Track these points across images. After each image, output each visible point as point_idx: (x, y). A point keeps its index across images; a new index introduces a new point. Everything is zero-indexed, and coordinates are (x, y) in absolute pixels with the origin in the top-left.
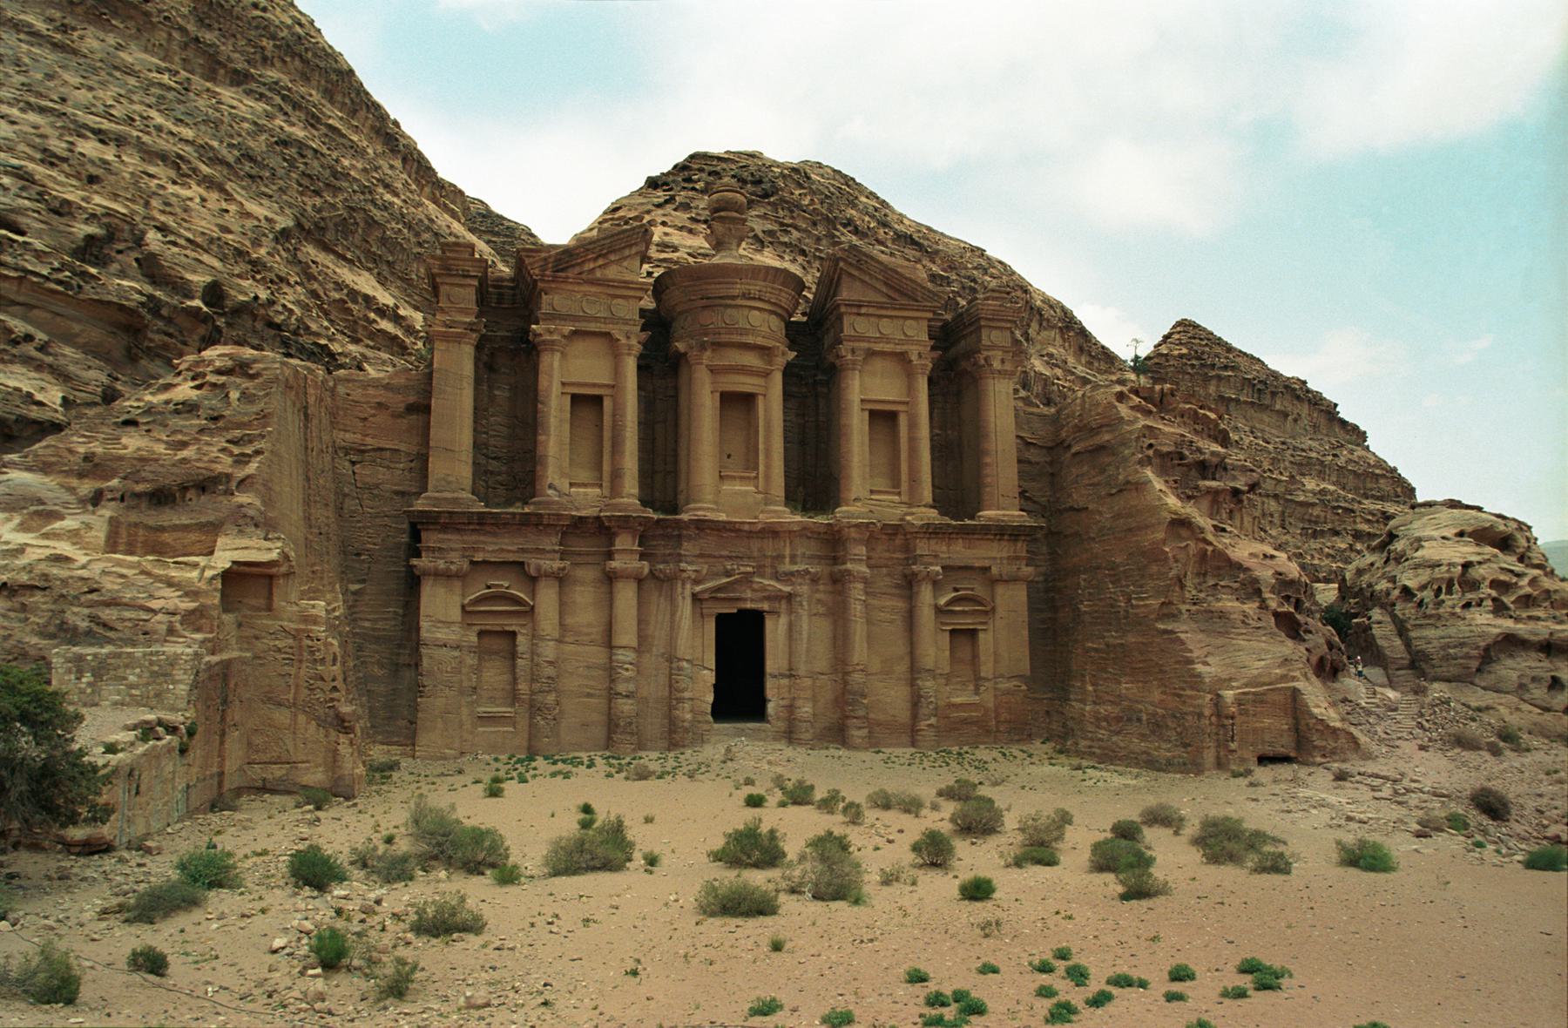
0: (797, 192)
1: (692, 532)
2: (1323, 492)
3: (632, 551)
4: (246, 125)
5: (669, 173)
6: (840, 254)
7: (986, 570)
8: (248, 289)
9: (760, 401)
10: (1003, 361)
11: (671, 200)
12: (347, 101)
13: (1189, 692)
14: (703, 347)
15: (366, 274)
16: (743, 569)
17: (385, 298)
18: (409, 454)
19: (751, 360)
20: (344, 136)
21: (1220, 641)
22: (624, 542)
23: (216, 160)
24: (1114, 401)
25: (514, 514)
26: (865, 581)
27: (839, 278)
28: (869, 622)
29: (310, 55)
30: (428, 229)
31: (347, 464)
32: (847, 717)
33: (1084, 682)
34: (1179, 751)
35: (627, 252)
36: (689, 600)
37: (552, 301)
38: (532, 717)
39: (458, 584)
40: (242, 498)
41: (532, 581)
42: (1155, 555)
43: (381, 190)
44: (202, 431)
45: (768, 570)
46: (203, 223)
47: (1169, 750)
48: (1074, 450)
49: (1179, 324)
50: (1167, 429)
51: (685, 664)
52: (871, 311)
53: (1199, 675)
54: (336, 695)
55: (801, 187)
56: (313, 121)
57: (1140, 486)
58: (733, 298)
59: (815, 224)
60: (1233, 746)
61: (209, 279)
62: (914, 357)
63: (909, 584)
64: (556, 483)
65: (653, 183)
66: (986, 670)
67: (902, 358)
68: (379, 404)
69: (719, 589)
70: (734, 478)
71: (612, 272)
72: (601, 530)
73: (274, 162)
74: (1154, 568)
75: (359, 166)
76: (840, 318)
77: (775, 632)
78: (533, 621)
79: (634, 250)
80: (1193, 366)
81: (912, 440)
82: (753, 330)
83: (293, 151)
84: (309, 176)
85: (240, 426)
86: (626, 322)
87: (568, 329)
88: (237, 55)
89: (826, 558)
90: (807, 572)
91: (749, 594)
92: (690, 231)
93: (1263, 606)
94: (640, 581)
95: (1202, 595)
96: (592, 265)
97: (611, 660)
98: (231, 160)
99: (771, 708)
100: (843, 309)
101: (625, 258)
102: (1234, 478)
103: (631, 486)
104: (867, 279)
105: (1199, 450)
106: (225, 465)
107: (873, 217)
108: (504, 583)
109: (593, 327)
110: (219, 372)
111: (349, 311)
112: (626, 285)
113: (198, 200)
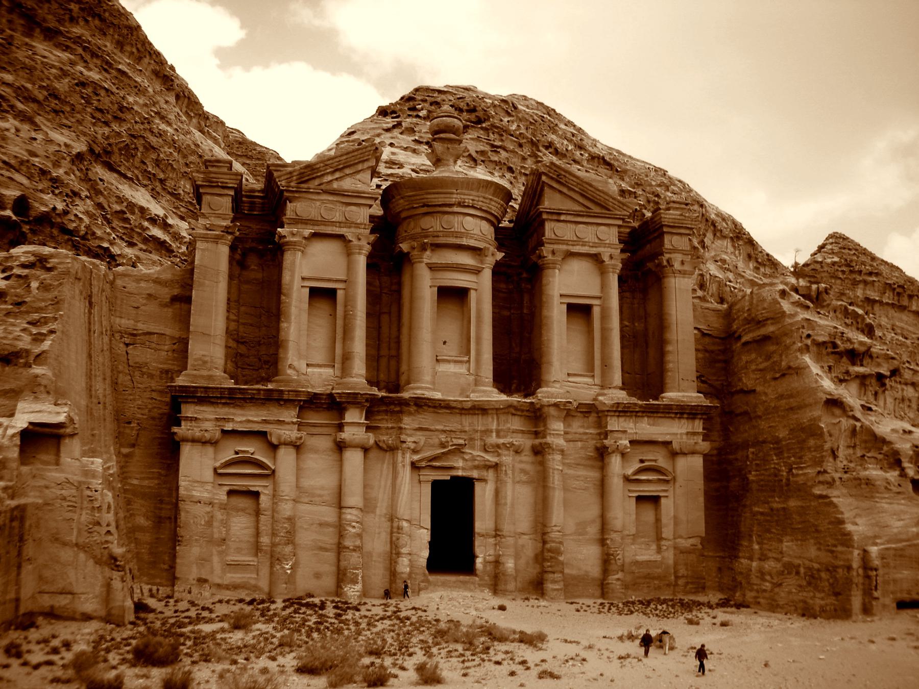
0: (506, 120)
1: (413, 409)
3: (359, 424)
4: (54, 71)
5: (397, 103)
6: (542, 169)
7: (667, 444)
8: (50, 202)
9: (473, 295)
10: (683, 263)
11: (399, 124)
12: (134, 50)
13: (840, 548)
14: (423, 248)
15: (143, 190)
16: (456, 441)
17: (157, 209)
18: (172, 338)
19: (465, 259)
20: (130, 78)
21: (866, 504)
22: (353, 416)
23: (29, 98)
24: (777, 297)
25: (259, 390)
26: (562, 452)
27: (542, 190)
28: (565, 489)
29: (107, 14)
30: (194, 152)
31: (122, 345)
32: (546, 572)
33: (751, 541)
34: (831, 600)
35: (360, 167)
36: (408, 468)
38: (272, 566)
39: (210, 450)
40: (37, 370)
41: (274, 448)
42: (813, 431)
43: (157, 121)
44: (8, 314)
45: (478, 443)
46: (17, 149)
47: (822, 599)
48: (744, 339)
49: (832, 236)
50: (822, 322)
51: (405, 524)
52: (569, 218)
53: (849, 534)
54: (110, 538)
55: (509, 114)
56: (107, 67)
57: (799, 371)
58: (451, 205)
59: (521, 146)
60: (876, 594)
61: (18, 193)
62: (606, 258)
63: (602, 454)
64: (295, 364)
65: (383, 112)
66: (668, 531)
67: (596, 258)
68: (150, 295)
69: (435, 458)
70: (448, 361)
71: (348, 184)
72: (332, 405)
73: (75, 99)
74: (812, 442)
75: (141, 102)
76: (542, 223)
77: (483, 496)
78: (275, 484)
79: (366, 165)
80: (843, 272)
81: (605, 331)
82: (467, 234)
83: (88, 91)
84: (101, 111)
85: (38, 310)
86: (357, 225)
87: (307, 232)
88: (50, 17)
89: (529, 432)
90: (512, 444)
91: (460, 463)
92: (414, 151)
93: (903, 474)
94: (366, 450)
95: (852, 465)
96: (330, 178)
97: (340, 517)
98: (41, 97)
99: (479, 562)
100: (545, 216)
101: (358, 172)
102: (879, 365)
103: (359, 367)
104: (565, 190)
105: (849, 340)
106: (25, 342)
107: (570, 141)
108: (251, 448)
109: (329, 230)
110: (23, 266)
111: (127, 220)
112: (358, 195)
113: (13, 131)
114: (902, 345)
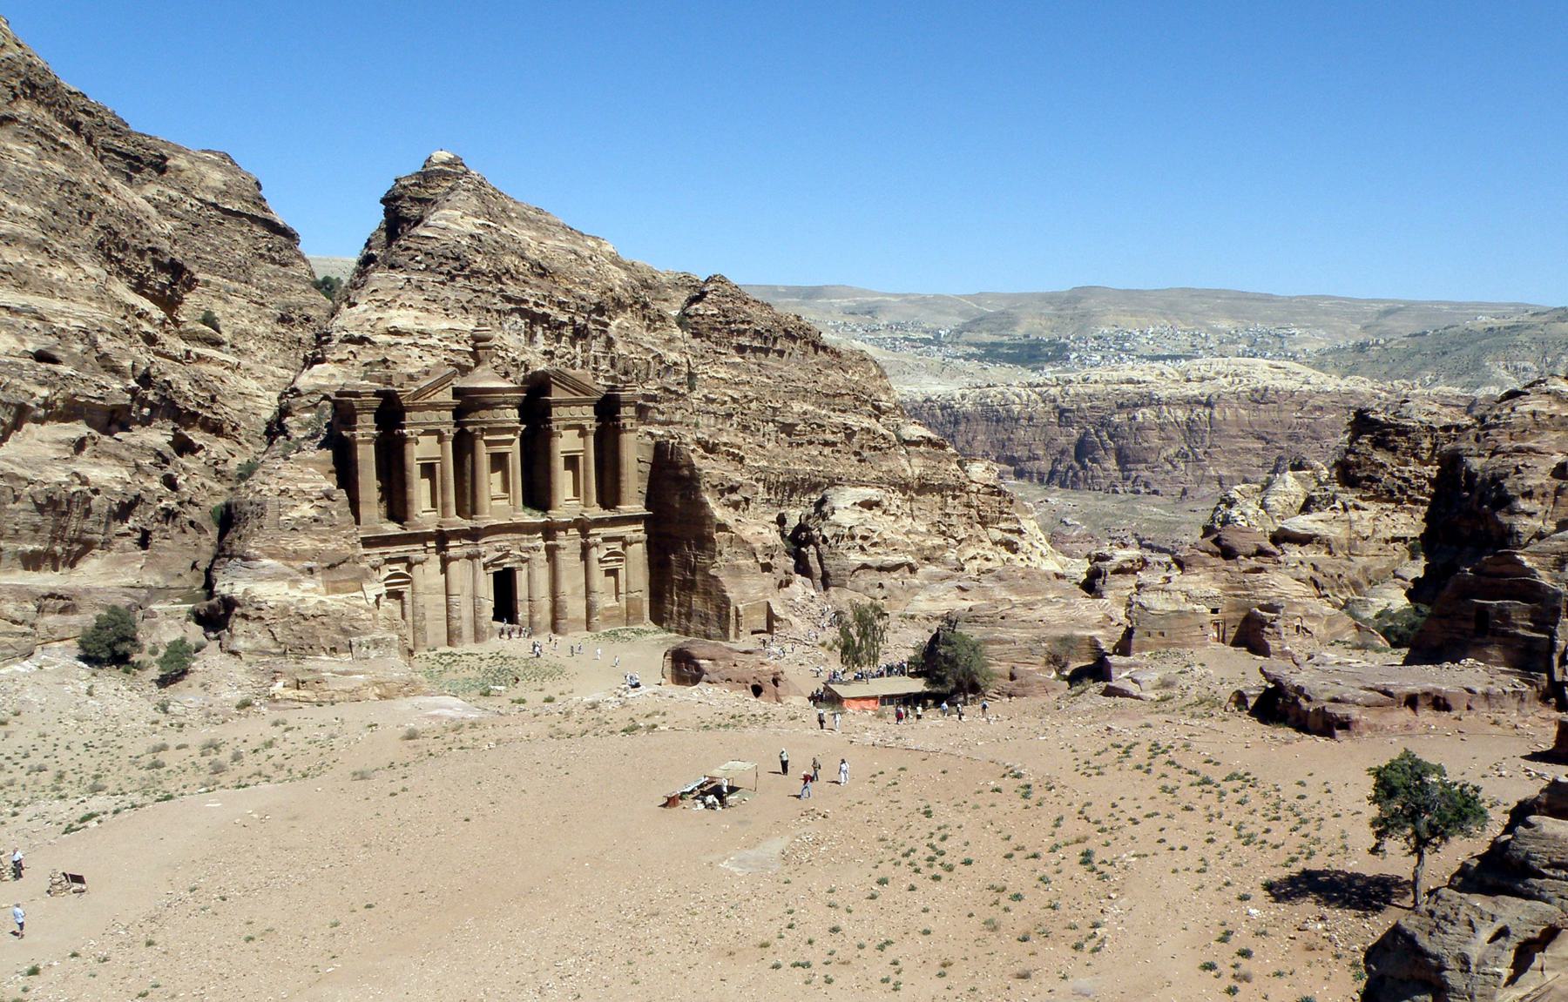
2: (805, 413)
37: (410, 417)
57: (704, 505)
77: (521, 578)
114: (767, 385)
